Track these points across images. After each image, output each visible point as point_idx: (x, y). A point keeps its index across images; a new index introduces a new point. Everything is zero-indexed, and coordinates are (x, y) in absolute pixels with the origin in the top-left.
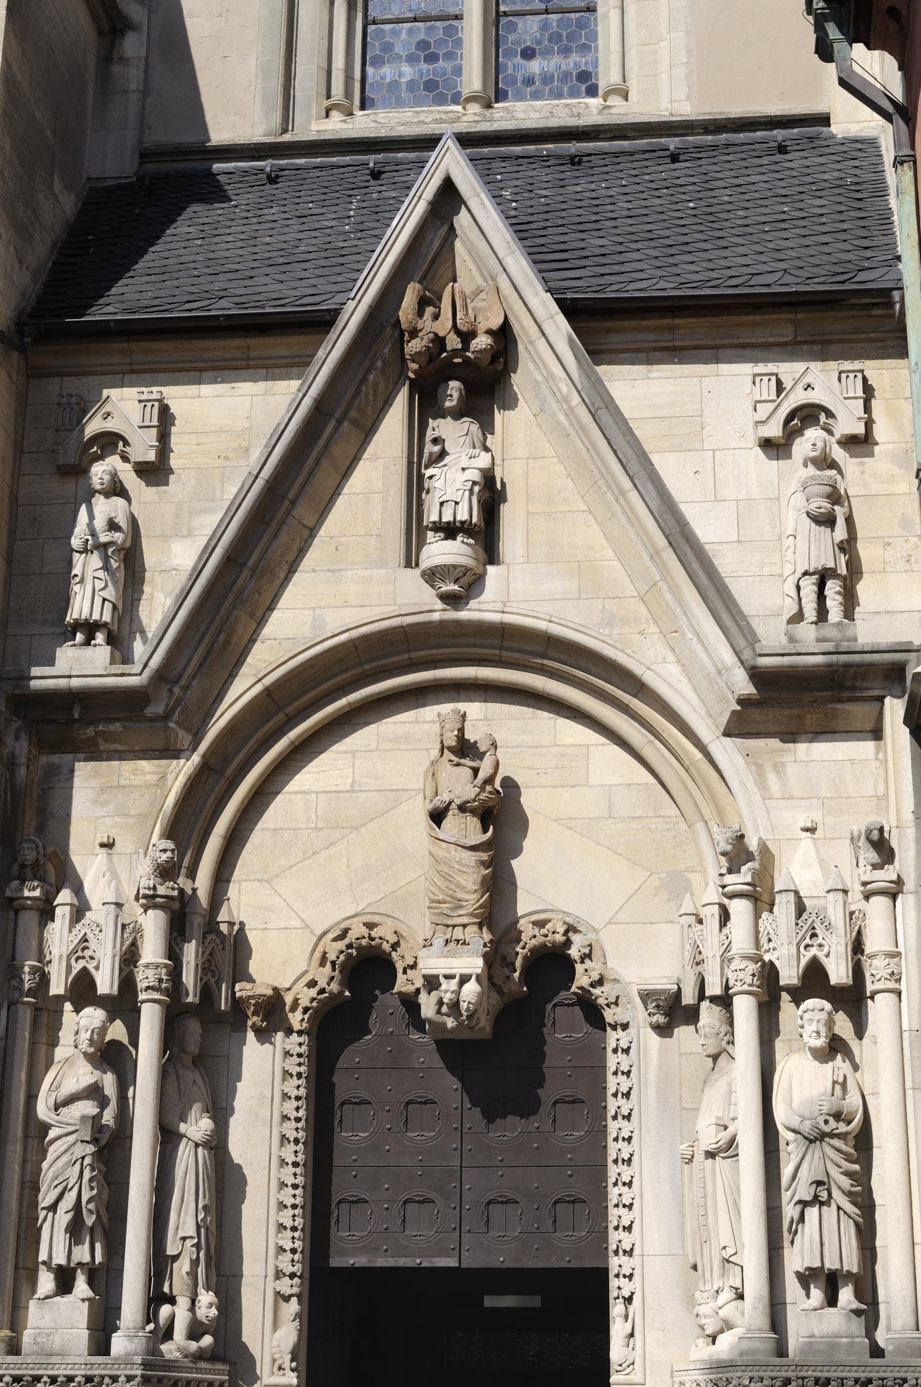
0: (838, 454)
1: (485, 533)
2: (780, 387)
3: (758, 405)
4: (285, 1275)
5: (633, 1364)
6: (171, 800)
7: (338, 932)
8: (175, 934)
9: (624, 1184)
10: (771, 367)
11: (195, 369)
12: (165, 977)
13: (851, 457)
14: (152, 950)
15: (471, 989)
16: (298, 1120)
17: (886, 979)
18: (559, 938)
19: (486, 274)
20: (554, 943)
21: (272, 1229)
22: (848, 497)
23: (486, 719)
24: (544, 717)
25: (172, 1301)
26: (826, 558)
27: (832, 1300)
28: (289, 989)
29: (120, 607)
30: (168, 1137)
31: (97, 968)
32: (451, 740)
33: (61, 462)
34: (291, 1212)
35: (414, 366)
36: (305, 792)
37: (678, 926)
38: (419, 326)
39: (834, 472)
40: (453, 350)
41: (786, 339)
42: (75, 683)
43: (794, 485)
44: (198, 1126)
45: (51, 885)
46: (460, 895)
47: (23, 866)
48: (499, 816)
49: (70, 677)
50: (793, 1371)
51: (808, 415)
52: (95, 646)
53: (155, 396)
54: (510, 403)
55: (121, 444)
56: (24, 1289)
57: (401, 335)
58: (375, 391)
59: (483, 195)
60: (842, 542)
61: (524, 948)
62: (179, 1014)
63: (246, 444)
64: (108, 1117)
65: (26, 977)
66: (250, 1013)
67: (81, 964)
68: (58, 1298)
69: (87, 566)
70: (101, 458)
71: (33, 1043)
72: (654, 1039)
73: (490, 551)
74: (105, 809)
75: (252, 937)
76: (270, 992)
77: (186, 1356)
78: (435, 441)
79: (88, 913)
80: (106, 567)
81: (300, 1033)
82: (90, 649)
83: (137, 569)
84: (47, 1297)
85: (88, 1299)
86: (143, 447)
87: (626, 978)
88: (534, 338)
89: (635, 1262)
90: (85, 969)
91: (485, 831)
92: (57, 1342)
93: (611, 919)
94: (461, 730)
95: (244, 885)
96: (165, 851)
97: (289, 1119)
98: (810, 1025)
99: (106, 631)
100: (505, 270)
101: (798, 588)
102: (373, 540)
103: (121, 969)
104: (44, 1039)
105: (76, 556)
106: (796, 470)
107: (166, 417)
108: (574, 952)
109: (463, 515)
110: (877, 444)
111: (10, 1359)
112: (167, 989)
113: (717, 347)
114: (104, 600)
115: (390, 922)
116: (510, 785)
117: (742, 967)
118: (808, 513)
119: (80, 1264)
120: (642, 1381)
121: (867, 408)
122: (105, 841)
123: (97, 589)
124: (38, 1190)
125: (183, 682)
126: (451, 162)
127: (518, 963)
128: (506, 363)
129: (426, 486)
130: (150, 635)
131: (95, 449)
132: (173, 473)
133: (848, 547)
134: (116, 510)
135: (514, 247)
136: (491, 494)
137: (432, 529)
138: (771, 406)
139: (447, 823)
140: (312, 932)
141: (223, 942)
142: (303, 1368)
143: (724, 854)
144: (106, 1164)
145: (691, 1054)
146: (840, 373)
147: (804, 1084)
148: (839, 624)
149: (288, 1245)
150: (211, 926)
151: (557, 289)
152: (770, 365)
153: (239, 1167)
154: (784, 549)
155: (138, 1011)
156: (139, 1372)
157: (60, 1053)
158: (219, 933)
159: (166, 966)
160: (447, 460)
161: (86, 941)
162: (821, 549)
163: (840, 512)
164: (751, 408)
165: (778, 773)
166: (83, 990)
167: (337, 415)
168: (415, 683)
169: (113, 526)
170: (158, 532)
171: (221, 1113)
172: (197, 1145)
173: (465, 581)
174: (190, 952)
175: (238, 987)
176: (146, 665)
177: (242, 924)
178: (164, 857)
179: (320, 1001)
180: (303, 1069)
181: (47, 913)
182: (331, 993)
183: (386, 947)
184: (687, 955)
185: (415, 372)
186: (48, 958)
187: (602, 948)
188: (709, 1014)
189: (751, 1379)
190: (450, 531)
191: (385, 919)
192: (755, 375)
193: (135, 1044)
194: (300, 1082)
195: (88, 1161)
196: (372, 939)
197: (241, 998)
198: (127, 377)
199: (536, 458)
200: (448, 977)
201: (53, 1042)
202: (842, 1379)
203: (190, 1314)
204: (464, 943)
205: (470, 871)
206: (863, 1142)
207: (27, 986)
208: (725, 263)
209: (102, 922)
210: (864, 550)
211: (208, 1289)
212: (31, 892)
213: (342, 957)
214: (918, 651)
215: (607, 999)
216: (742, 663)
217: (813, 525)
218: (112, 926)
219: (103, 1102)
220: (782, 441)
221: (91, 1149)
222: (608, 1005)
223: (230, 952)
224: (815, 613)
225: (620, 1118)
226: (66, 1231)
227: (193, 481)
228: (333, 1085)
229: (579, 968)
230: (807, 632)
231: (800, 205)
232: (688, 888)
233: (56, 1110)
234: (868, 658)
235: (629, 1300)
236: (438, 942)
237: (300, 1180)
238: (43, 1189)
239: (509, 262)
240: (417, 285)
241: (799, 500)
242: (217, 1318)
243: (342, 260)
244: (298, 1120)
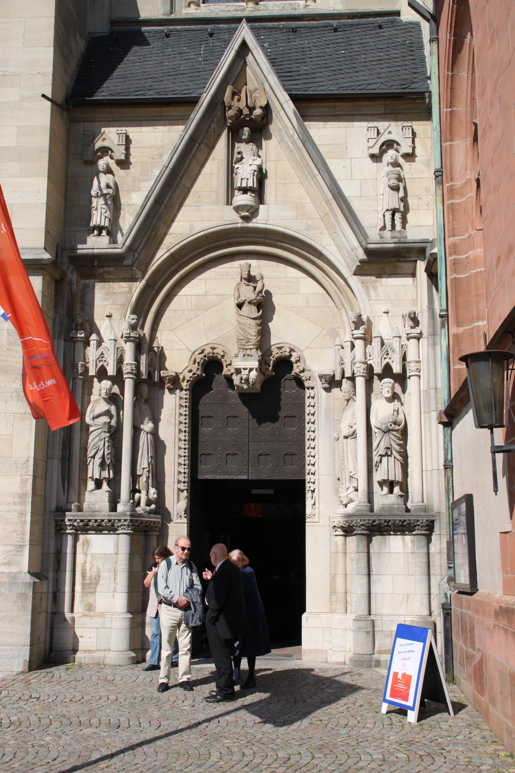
0: (401, 161)
1: (259, 191)
2: (378, 133)
3: (370, 140)
4: (181, 482)
6: (134, 298)
7: (200, 351)
8: (137, 352)
9: (312, 448)
10: (375, 124)
11: (139, 120)
12: (134, 369)
13: (406, 162)
14: (129, 358)
15: (254, 374)
16: (186, 423)
18: (287, 354)
19: (259, 82)
20: (285, 356)
21: (176, 465)
22: (404, 179)
23: (258, 267)
24: (282, 266)
25: (139, 491)
26: (395, 204)
27: (391, 491)
28: (181, 373)
29: (112, 220)
30: (136, 430)
31: (107, 365)
32: (245, 275)
33: (86, 159)
34: (183, 458)
35: (230, 121)
36: (186, 295)
37: (334, 350)
38: (232, 105)
39: (399, 168)
40: (246, 115)
41: (381, 112)
42: (95, 251)
43: (383, 173)
44: (147, 426)
45: (87, 332)
46: (249, 337)
47: (77, 325)
48: (264, 305)
49: (93, 249)
51: (389, 144)
52: (103, 236)
53: (124, 132)
54: (269, 137)
55: (110, 152)
56: (83, 488)
57: (225, 108)
58: (214, 132)
59: (258, 48)
60: (402, 197)
61: (273, 357)
62: (139, 383)
63: (161, 152)
64: (113, 422)
65: (80, 368)
66: (166, 382)
67: (101, 363)
68: (96, 491)
69: (98, 203)
70: (101, 157)
71: (83, 394)
72: (324, 393)
73: (261, 200)
74: (108, 302)
75: (166, 352)
76: (174, 374)
77: (145, 512)
78: (239, 153)
79: (103, 343)
80: (106, 204)
81: (186, 390)
82: (101, 238)
83: (118, 204)
84: (92, 490)
85: (108, 491)
86: (119, 153)
88: (279, 110)
90: (103, 366)
91: (259, 312)
92: (97, 507)
94: (249, 271)
95: (163, 332)
96: (133, 319)
97: (182, 423)
99: (106, 230)
100: (267, 81)
101: (384, 216)
102: (214, 194)
103: (117, 366)
104: (86, 392)
105: (93, 199)
106: (384, 168)
107: (128, 141)
108: (293, 359)
109: (250, 184)
110: (416, 157)
111: (79, 513)
112: (135, 373)
113: (353, 115)
114: (106, 217)
115: (221, 347)
116: (268, 293)
118: (389, 186)
119: (105, 478)
121: (413, 142)
122: (108, 314)
123: (102, 213)
124: (87, 450)
125: (138, 251)
126: (245, 33)
127: (271, 363)
128: (267, 120)
129: (235, 171)
130: (125, 232)
131: (99, 154)
132: (131, 164)
133: (404, 200)
134: (109, 180)
135: (271, 71)
136: (261, 175)
137: (237, 190)
138: (375, 141)
139: (244, 308)
140: (190, 351)
141: (156, 355)
142: (188, 517)
143: (353, 322)
144: (113, 440)
146: (403, 127)
147: (382, 411)
148: (400, 231)
149: (183, 471)
150: (151, 349)
151: (289, 89)
152: (375, 123)
153: (163, 441)
154: (379, 200)
155: (124, 382)
156: (129, 518)
157: (93, 398)
158: (154, 351)
159: (135, 364)
160: (244, 161)
161: (103, 354)
162: (393, 200)
163: (401, 185)
164: (367, 141)
165: (374, 290)
166: (102, 374)
167: (199, 141)
168: (230, 252)
169: (108, 186)
170: (126, 189)
171: (156, 421)
172: (147, 433)
173: (251, 211)
174: (143, 359)
175: (162, 372)
176: (124, 244)
177: (162, 347)
178: (133, 321)
179: (193, 378)
180: (187, 404)
181: (87, 343)
182: (198, 375)
183: (219, 357)
184: (338, 361)
185: (230, 124)
186: (87, 361)
187: (304, 358)
188: (346, 384)
189: (361, 520)
190: (245, 190)
191: (219, 346)
192: (368, 127)
193: (123, 395)
194: (186, 409)
195: (107, 439)
196: (214, 354)
197: (163, 376)
198: (111, 123)
199: (279, 161)
200: (244, 369)
201: (90, 393)
202: (395, 520)
203: (146, 497)
204: (251, 356)
205: (253, 328)
206: (404, 433)
207: (80, 372)
208: (357, 79)
209: (109, 347)
210: (410, 200)
211: (153, 487)
212: (81, 335)
213: (202, 361)
214: (431, 242)
216: (362, 246)
217: (391, 190)
218: (113, 349)
219: (111, 417)
220: (379, 155)
221: (108, 435)
222: (306, 380)
223: (158, 359)
224: (390, 227)
225: (310, 423)
226: (99, 466)
227: (140, 168)
228: (198, 410)
229: (295, 366)
230: (387, 234)
231: (388, 53)
232: (338, 335)
233: (93, 419)
234: (411, 245)
235: (313, 491)
237: (187, 446)
238: (89, 450)
239: (269, 78)
240: (231, 87)
241: (385, 180)
242: (156, 499)
243: (199, 74)
244: (186, 423)
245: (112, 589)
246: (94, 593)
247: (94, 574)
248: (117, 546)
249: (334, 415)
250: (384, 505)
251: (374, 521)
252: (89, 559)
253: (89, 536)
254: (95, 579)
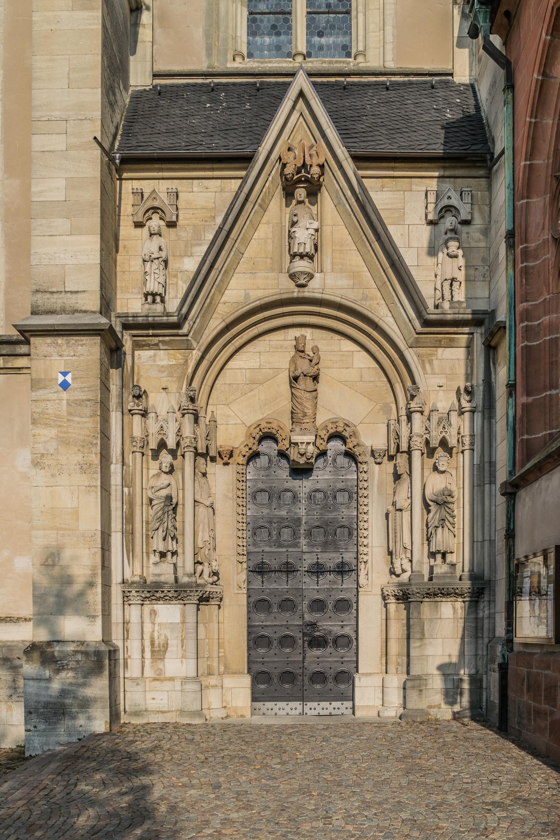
63: (213, 214)
89: (369, 550)
102: (269, 260)
236: (297, 429)
245: (180, 655)
246: (163, 659)
247: (162, 643)
248: (183, 616)
252: (157, 628)
253: (156, 606)
254: (163, 646)
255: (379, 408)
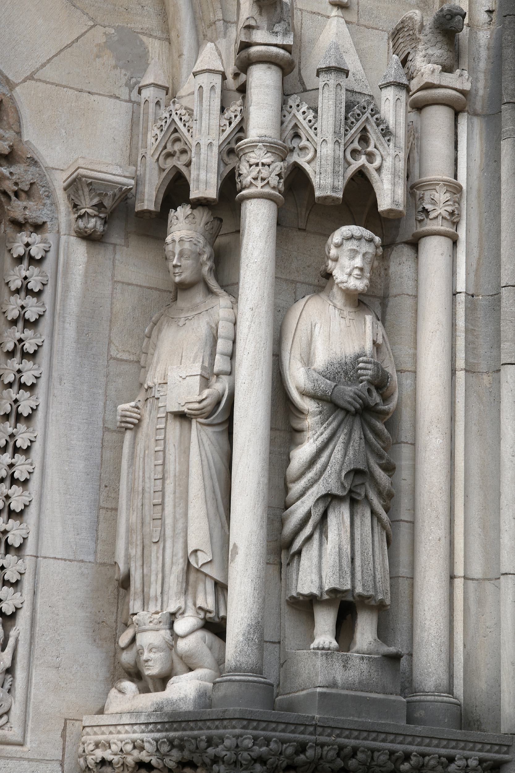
5: (7, 713)
17: (443, 218)
50: (311, 734)
72: (79, 251)
87: (48, 160)
93: (34, 73)
98: (353, 258)
117: (266, 160)
120: (19, 739)
145: (129, 284)
147: (329, 336)
187: (17, 111)
189: (255, 738)
202: (373, 751)
215: (16, 184)
249: (110, 342)
250: (334, 685)
251: (302, 748)
255: (102, 40)
